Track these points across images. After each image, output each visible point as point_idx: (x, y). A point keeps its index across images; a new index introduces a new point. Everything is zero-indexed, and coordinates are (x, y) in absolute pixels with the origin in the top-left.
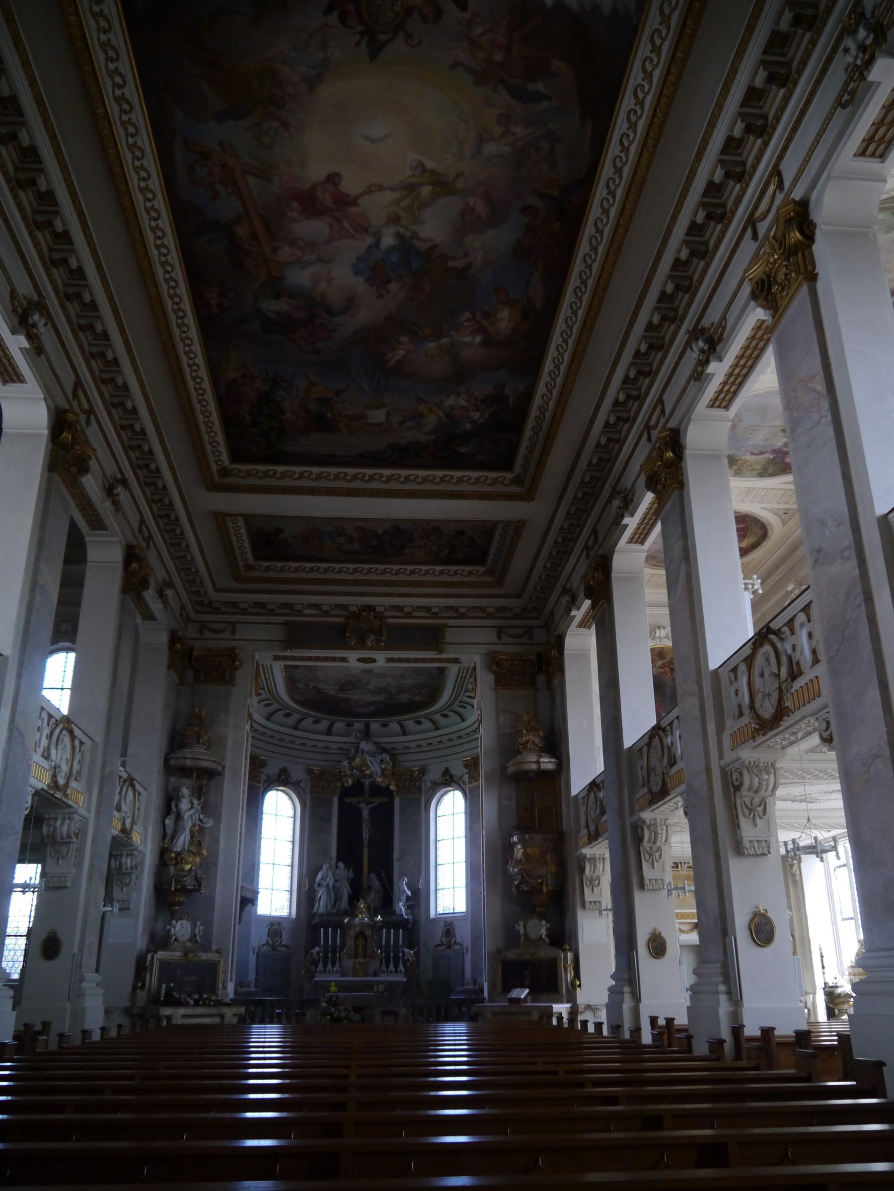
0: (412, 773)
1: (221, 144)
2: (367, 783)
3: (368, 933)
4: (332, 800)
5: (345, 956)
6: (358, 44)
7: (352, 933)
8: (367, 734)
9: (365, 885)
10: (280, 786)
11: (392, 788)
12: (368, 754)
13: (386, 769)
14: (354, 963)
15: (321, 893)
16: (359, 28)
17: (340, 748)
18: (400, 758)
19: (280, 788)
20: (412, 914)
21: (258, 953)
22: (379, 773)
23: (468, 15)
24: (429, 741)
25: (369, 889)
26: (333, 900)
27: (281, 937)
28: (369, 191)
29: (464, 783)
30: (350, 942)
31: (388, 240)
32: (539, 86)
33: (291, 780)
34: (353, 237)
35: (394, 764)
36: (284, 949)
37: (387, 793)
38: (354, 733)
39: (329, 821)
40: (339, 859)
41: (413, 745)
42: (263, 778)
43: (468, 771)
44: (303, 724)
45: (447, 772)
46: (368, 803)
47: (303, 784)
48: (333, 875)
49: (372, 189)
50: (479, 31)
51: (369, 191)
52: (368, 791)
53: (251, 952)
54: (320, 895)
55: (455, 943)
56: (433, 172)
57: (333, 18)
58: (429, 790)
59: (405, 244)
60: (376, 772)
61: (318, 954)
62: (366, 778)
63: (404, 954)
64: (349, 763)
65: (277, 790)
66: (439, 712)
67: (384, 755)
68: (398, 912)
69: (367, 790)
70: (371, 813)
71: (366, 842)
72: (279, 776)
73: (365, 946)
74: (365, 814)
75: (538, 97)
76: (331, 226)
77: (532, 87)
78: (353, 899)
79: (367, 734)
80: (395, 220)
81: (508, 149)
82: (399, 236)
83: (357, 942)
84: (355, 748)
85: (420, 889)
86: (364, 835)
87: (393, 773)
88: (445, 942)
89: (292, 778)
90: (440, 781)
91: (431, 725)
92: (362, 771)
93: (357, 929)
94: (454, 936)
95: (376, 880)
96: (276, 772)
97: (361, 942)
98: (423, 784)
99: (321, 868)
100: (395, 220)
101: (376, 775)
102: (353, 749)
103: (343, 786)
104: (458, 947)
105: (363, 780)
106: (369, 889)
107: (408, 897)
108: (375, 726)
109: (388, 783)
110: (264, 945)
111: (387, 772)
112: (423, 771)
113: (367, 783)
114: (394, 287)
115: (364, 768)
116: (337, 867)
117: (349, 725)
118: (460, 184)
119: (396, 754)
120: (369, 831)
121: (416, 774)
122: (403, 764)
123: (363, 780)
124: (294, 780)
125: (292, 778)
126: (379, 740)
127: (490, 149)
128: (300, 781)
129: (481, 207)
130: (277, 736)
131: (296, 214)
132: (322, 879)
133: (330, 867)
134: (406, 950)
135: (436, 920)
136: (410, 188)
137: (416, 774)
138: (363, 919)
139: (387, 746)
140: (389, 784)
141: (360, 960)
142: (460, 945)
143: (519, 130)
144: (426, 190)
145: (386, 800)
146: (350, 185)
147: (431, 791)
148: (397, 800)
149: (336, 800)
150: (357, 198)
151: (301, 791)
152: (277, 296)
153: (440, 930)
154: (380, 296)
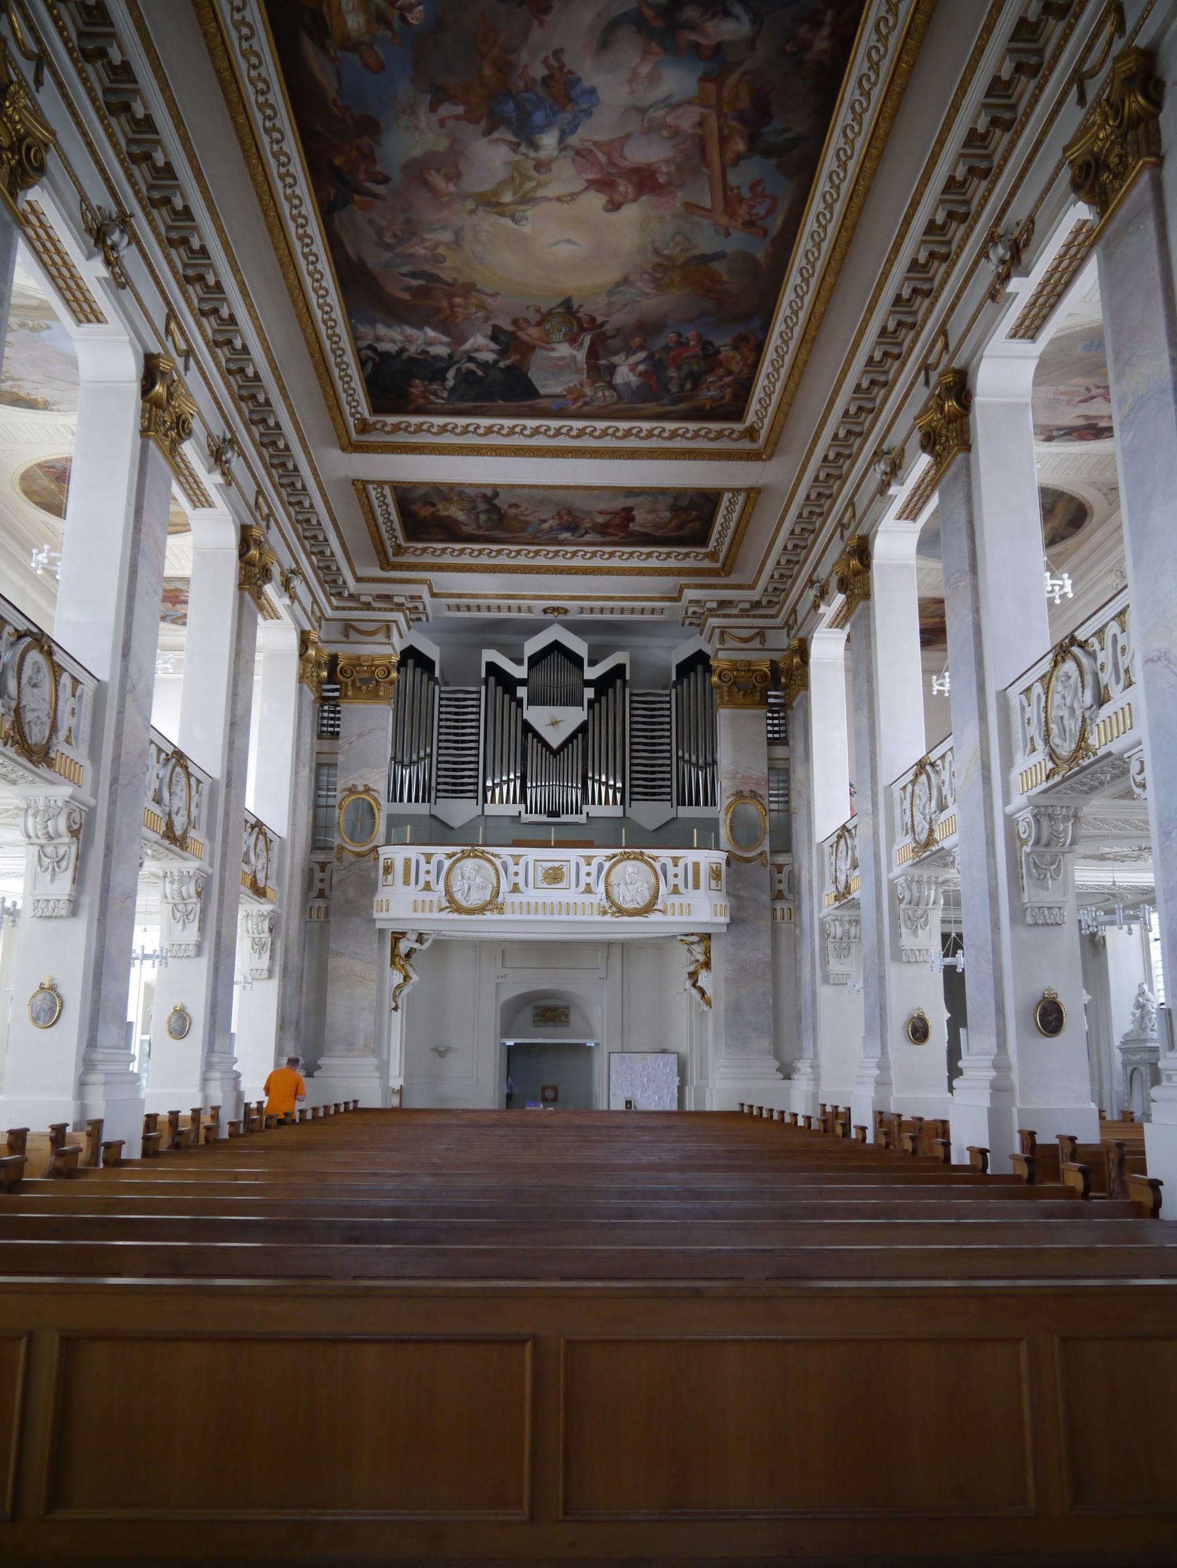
1: (728, 234)
6: (581, 306)
16: (580, 315)
23: (491, 323)
28: (573, 196)
31: (549, 140)
32: (415, 283)
34: (595, 143)
49: (569, 198)
50: (479, 314)
51: (573, 196)
56: (503, 215)
57: (600, 320)
59: (526, 134)
75: (413, 275)
76: (622, 157)
77: (421, 282)
80: (540, 166)
81: (427, 236)
82: (535, 146)
100: (540, 166)
114: (538, 71)
118: (470, 205)
127: (447, 236)
129: (439, 182)
131: (664, 169)
136: (526, 199)
143: (421, 251)
144: (507, 198)
146: (596, 201)
150: (586, 189)
152: (719, 47)
154: (558, 53)
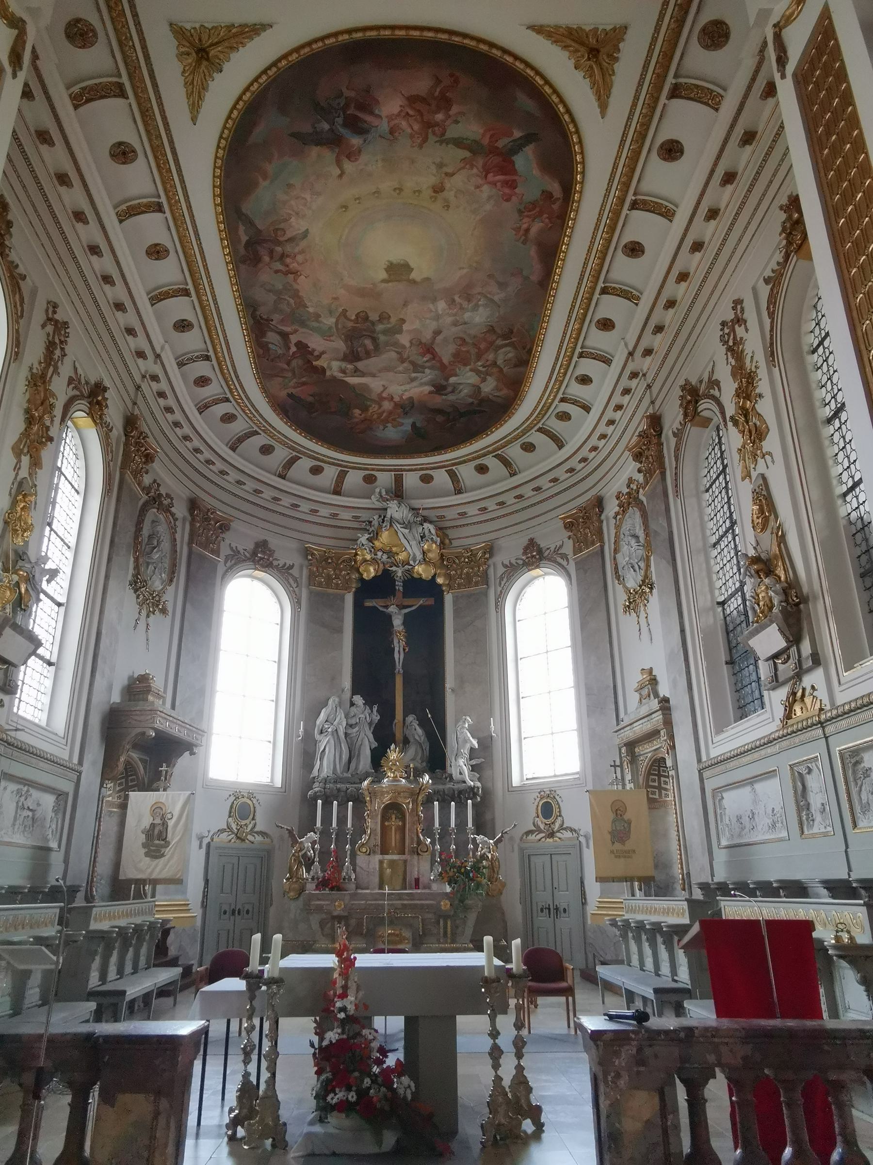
0: (474, 555)
2: (399, 574)
3: (407, 805)
4: (342, 599)
5: (364, 850)
7: (377, 806)
8: (398, 493)
9: (399, 736)
10: (256, 569)
11: (440, 581)
12: (400, 524)
13: (429, 551)
14: (381, 862)
15: (325, 742)
17: (356, 518)
18: (452, 534)
19: (258, 573)
20: (479, 780)
21: (209, 845)
22: (419, 556)
24: (500, 499)
25: (406, 741)
26: (345, 756)
27: (253, 819)
29: (564, 556)
30: (373, 824)
33: (275, 563)
35: (442, 542)
36: (259, 838)
37: (431, 588)
38: (377, 490)
39: (340, 630)
40: (354, 692)
41: (472, 510)
42: (225, 551)
43: (570, 534)
44: (292, 473)
45: (532, 544)
46: (401, 607)
47: (295, 572)
48: (347, 716)
52: (401, 588)
53: (195, 843)
54: (321, 750)
55: (562, 828)
58: (501, 578)
60: (414, 555)
61: (314, 843)
62: (398, 567)
63: (476, 846)
64: (370, 540)
65: (250, 576)
66: (524, 433)
67: (426, 525)
68: (456, 775)
69: (399, 586)
70: (408, 620)
71: (399, 667)
72: (254, 554)
73: (402, 829)
74: (398, 622)
78: (378, 756)
79: (398, 493)
83: (386, 823)
84: (380, 516)
85: (492, 737)
86: (396, 656)
87: (442, 555)
88: (542, 826)
89: (276, 559)
90: (521, 562)
91: (503, 471)
92: (390, 554)
93: (387, 799)
94: (560, 816)
95: (418, 728)
96: (251, 546)
97: (394, 823)
98: (491, 572)
99: (325, 704)
101: (415, 561)
102: (376, 517)
103: (362, 580)
104: (568, 834)
105: (394, 568)
106: (406, 741)
107: (472, 749)
108: (411, 480)
109: (433, 572)
110: (222, 831)
111: (430, 555)
112: (490, 550)
113: (399, 574)
115: (394, 549)
116: (352, 704)
117: (370, 479)
119: (446, 528)
120: (404, 650)
121: (480, 554)
122: (455, 543)
123: (394, 568)
124: (281, 563)
125: (276, 559)
126: (416, 503)
128: (291, 567)
130: (250, 485)
132: (326, 721)
133: (340, 704)
134: (480, 838)
135: (522, 790)
137: (480, 554)
138: (395, 779)
139: (432, 514)
140: (435, 575)
141: (395, 857)
142: (572, 830)
145: (431, 601)
147: (505, 580)
148: (448, 599)
149: (349, 599)
151: (291, 580)
153: (532, 807)
